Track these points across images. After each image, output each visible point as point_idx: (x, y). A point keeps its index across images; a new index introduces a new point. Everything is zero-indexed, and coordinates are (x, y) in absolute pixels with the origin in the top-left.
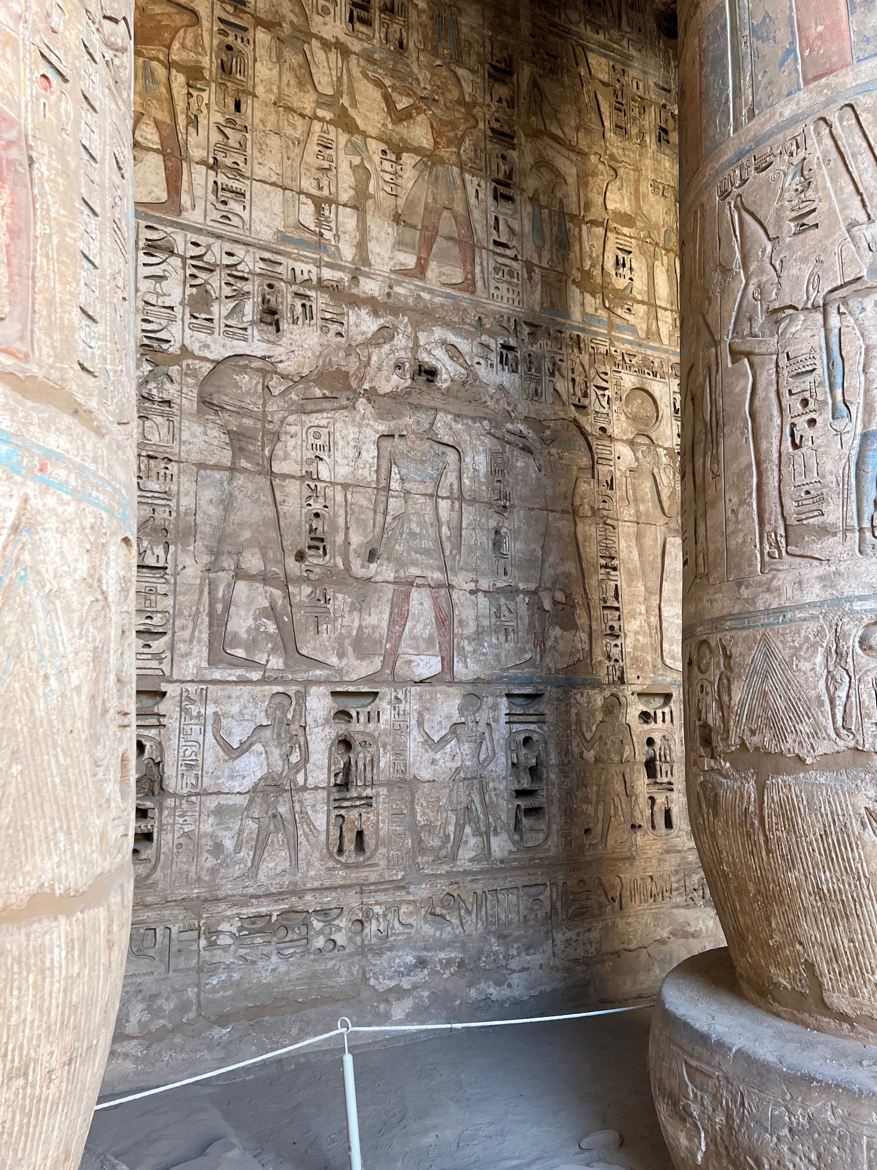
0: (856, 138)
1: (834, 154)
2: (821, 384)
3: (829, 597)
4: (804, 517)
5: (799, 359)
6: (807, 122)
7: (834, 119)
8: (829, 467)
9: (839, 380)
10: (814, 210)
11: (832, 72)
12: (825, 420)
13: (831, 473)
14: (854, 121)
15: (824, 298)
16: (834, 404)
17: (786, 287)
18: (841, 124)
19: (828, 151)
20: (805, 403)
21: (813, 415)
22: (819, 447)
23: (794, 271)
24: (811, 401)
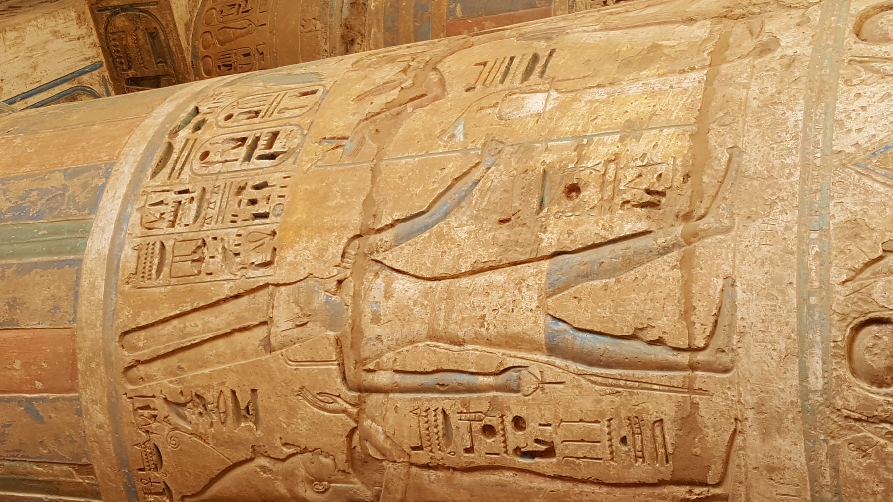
0: (164, 332)
1: (173, 361)
2: (465, 404)
3: (799, 425)
4: (661, 451)
5: (423, 431)
6: (121, 391)
7: (129, 357)
8: (588, 404)
9: (465, 378)
10: (233, 392)
11: (74, 354)
12: (518, 403)
13: (598, 402)
14: (143, 333)
15: (350, 389)
16: (498, 389)
17: (321, 441)
18: (140, 349)
19: (166, 369)
20: (488, 430)
21: (509, 419)
22: (556, 417)
23: (303, 427)
24: (487, 421)
